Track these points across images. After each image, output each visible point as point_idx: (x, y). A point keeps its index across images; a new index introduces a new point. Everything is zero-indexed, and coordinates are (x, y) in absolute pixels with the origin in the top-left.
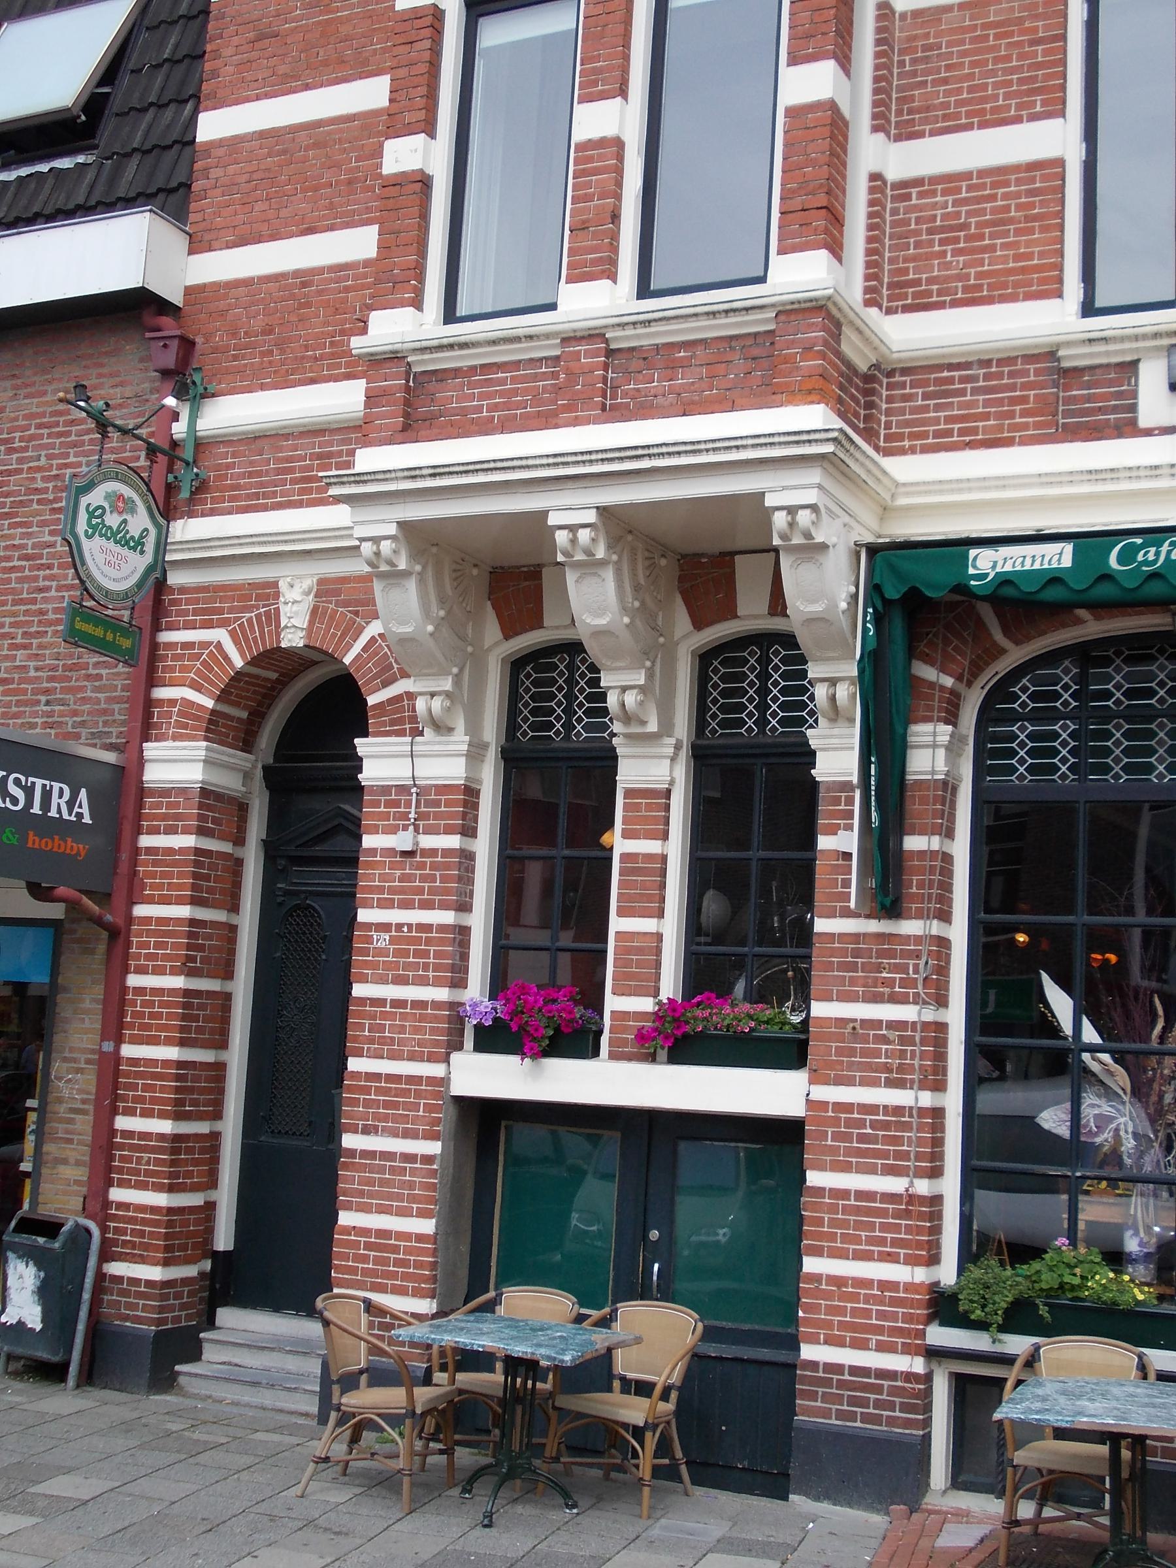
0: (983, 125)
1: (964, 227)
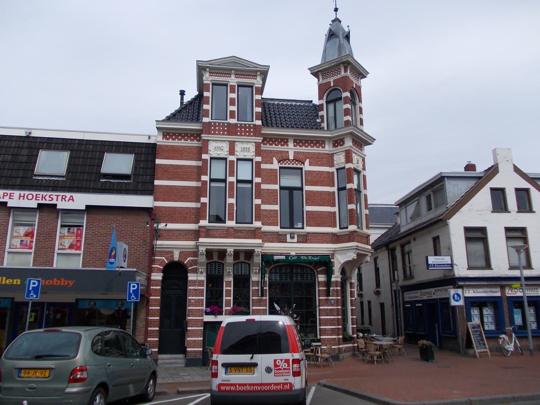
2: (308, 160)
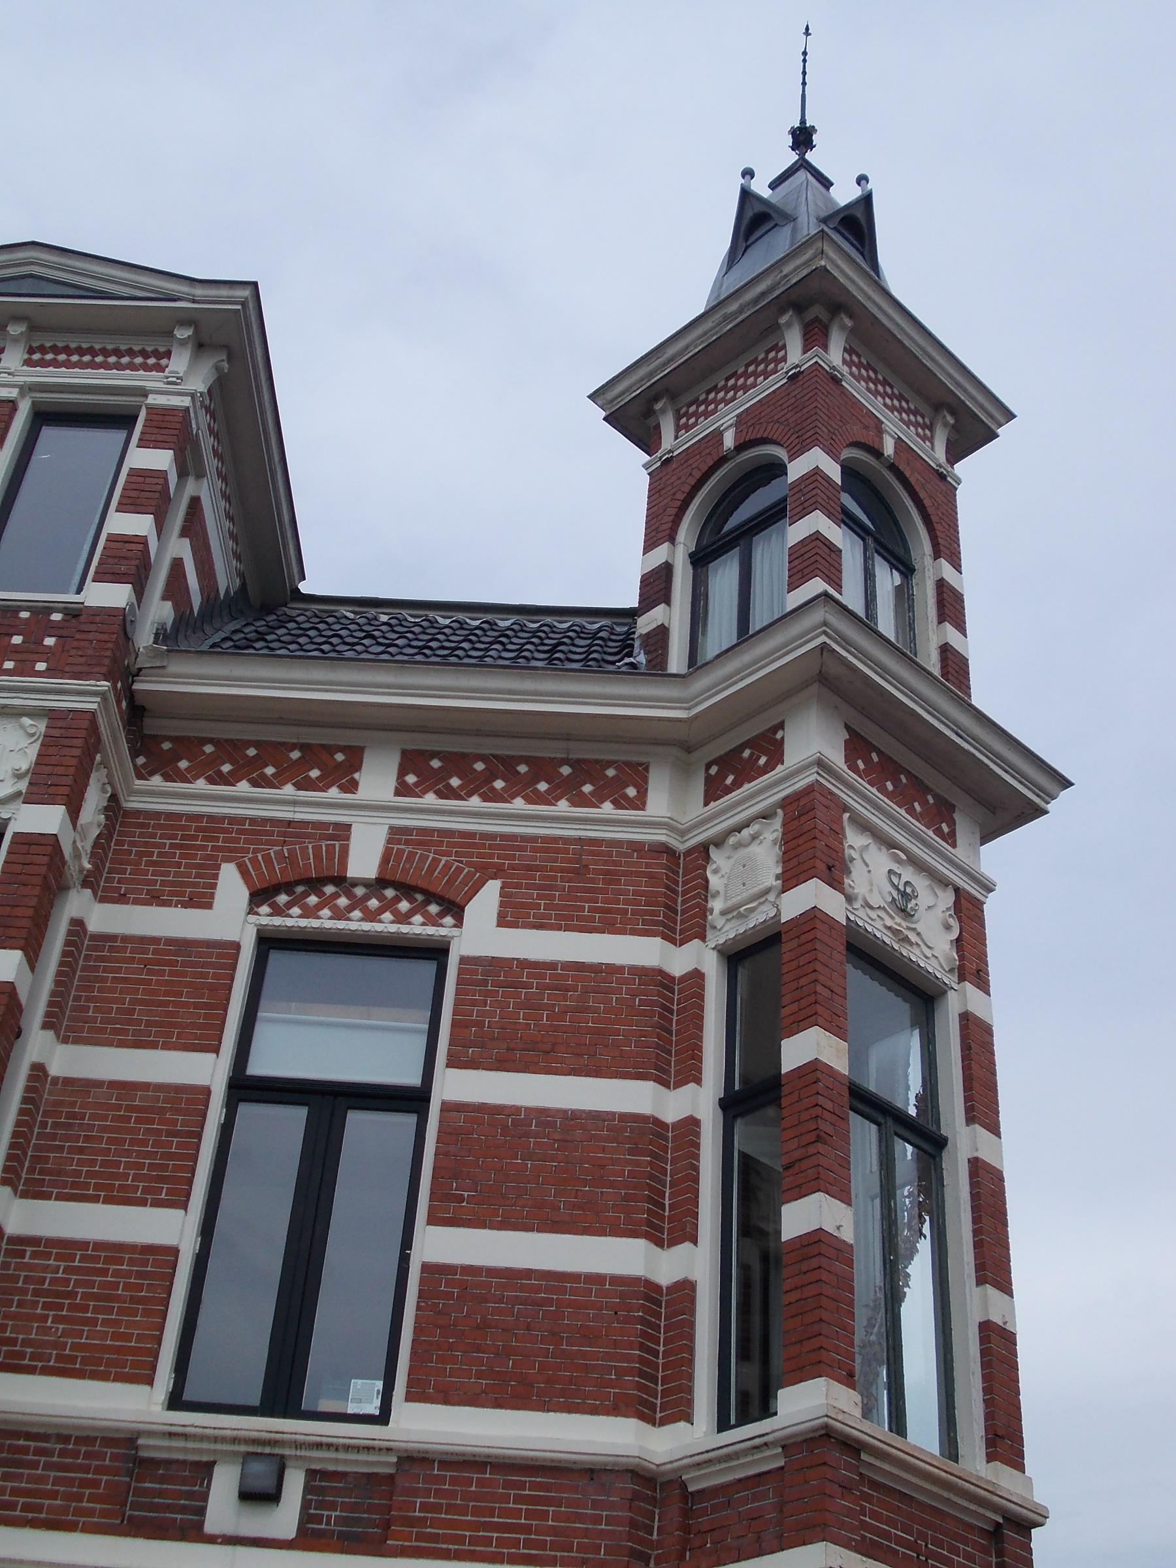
0: (109, 1200)
1: (71, 1295)
2: (492, 890)
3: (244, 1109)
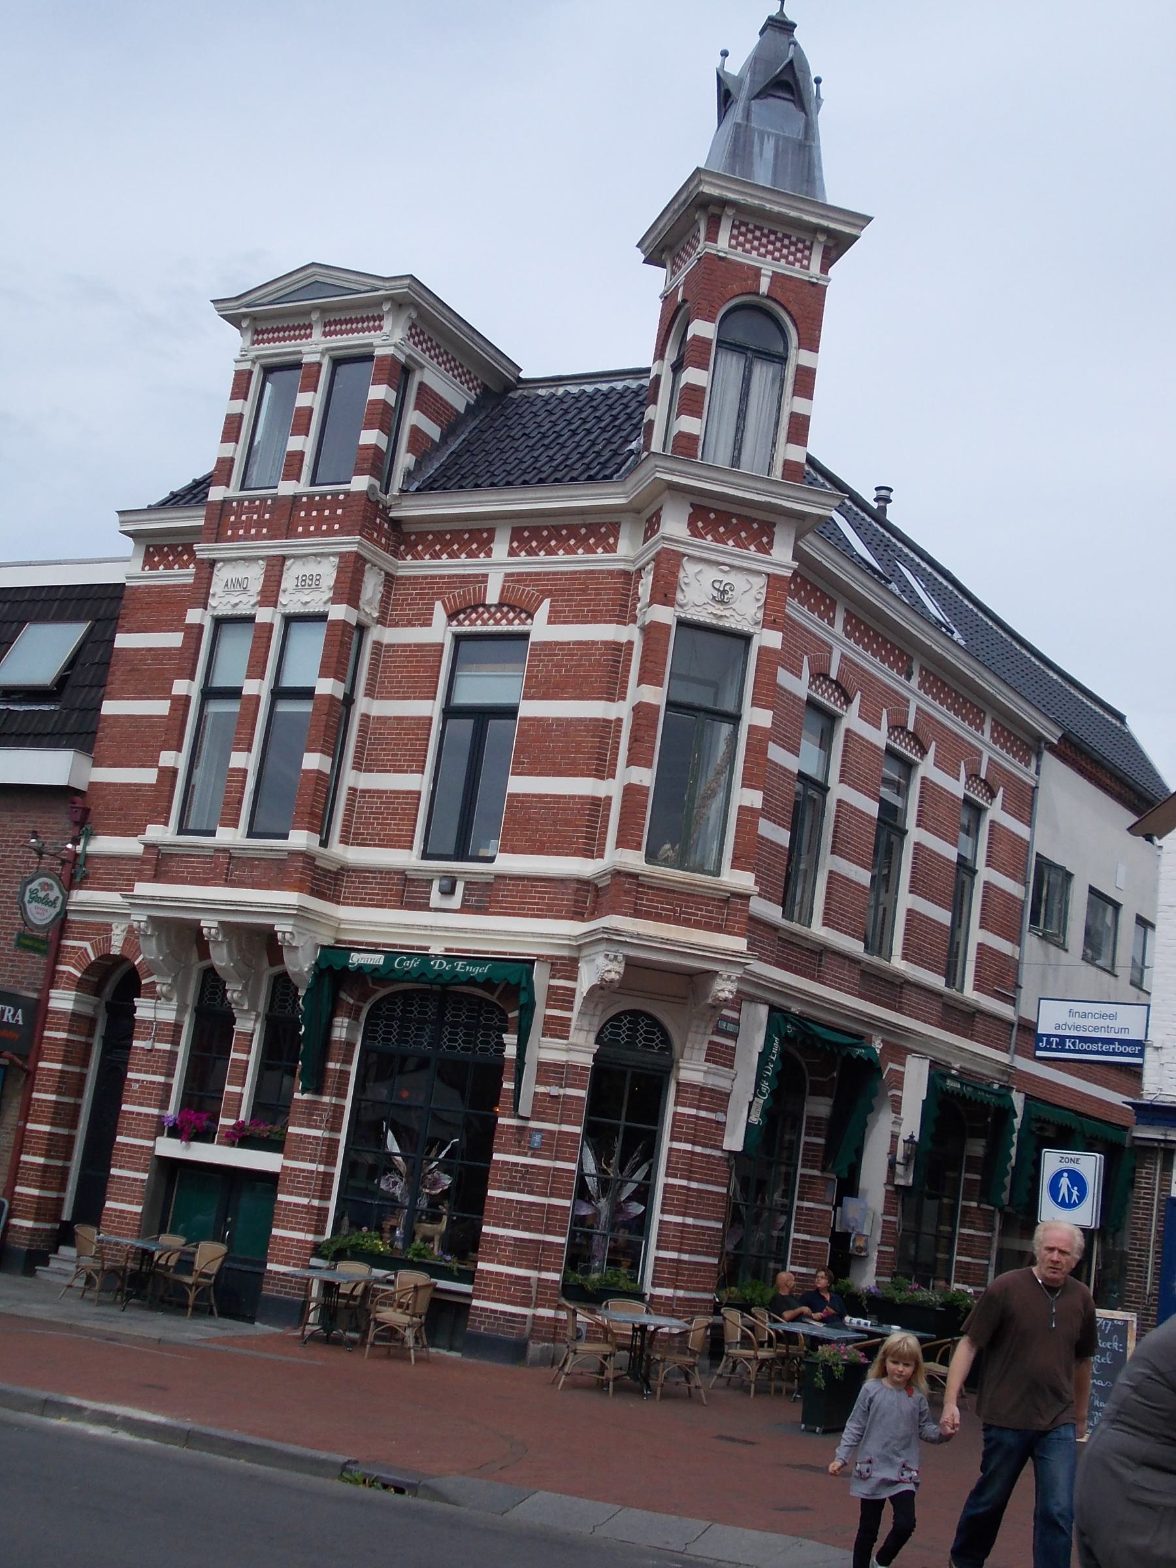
0: (396, 771)
1: (382, 813)
2: (547, 602)
3: (449, 722)
